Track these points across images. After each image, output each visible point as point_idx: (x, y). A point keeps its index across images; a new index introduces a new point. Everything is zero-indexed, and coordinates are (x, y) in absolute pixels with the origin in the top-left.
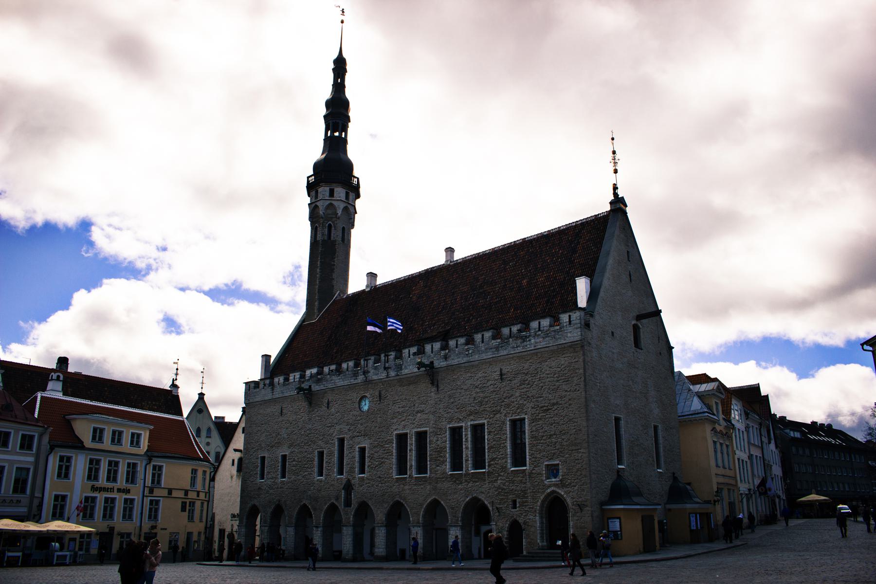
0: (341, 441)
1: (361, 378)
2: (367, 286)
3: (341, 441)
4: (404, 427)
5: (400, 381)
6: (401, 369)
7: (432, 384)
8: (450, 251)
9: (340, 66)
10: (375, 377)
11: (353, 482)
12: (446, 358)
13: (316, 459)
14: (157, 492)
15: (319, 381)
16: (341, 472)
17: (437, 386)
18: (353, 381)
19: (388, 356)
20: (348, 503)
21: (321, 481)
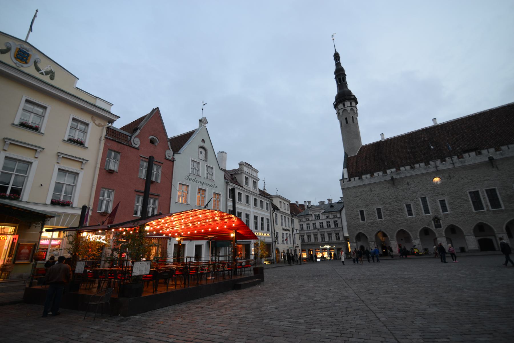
0: (424, 200)
1: (432, 170)
2: (382, 139)
3: (424, 200)
4: (475, 188)
5: (464, 168)
6: (465, 162)
7: (493, 167)
8: (434, 119)
9: (337, 57)
10: (443, 168)
11: (439, 216)
12: (501, 154)
13: (406, 208)
14: (295, 231)
15: (398, 173)
16: (427, 211)
17: (497, 168)
18: (426, 171)
19: (451, 158)
20: (438, 226)
21: (413, 218)
